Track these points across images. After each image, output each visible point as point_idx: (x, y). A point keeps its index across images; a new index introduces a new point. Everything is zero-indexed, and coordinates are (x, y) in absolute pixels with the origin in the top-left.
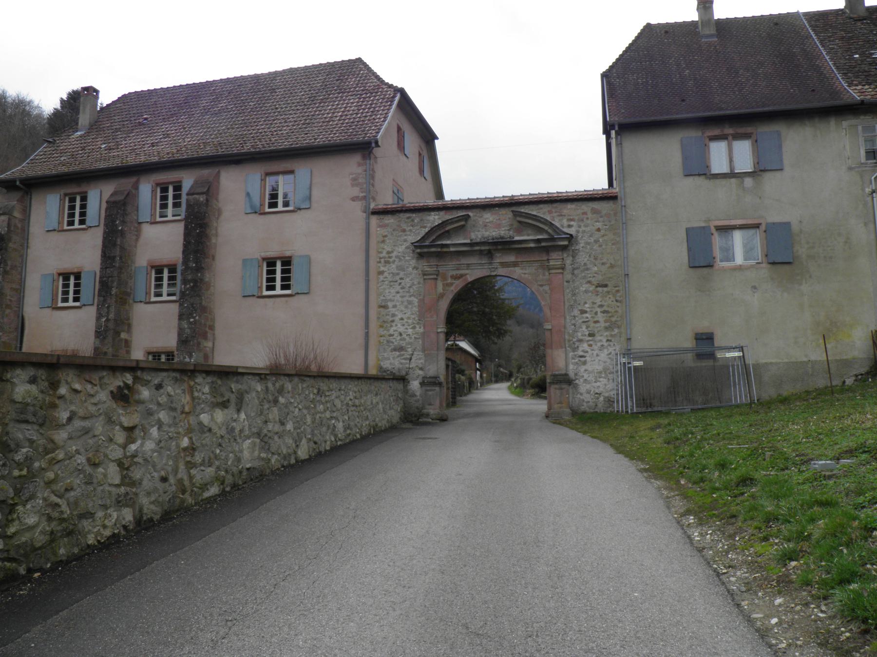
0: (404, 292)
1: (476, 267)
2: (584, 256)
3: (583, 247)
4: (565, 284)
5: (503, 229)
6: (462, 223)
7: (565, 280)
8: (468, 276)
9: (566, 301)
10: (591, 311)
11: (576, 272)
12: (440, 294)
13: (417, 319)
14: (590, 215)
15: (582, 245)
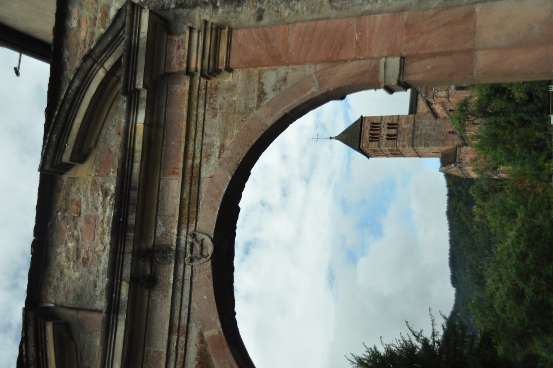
1: (186, 303)
4: (266, 20)
5: (100, 210)
6: (49, 328)
7: (253, 22)
9: (315, 16)
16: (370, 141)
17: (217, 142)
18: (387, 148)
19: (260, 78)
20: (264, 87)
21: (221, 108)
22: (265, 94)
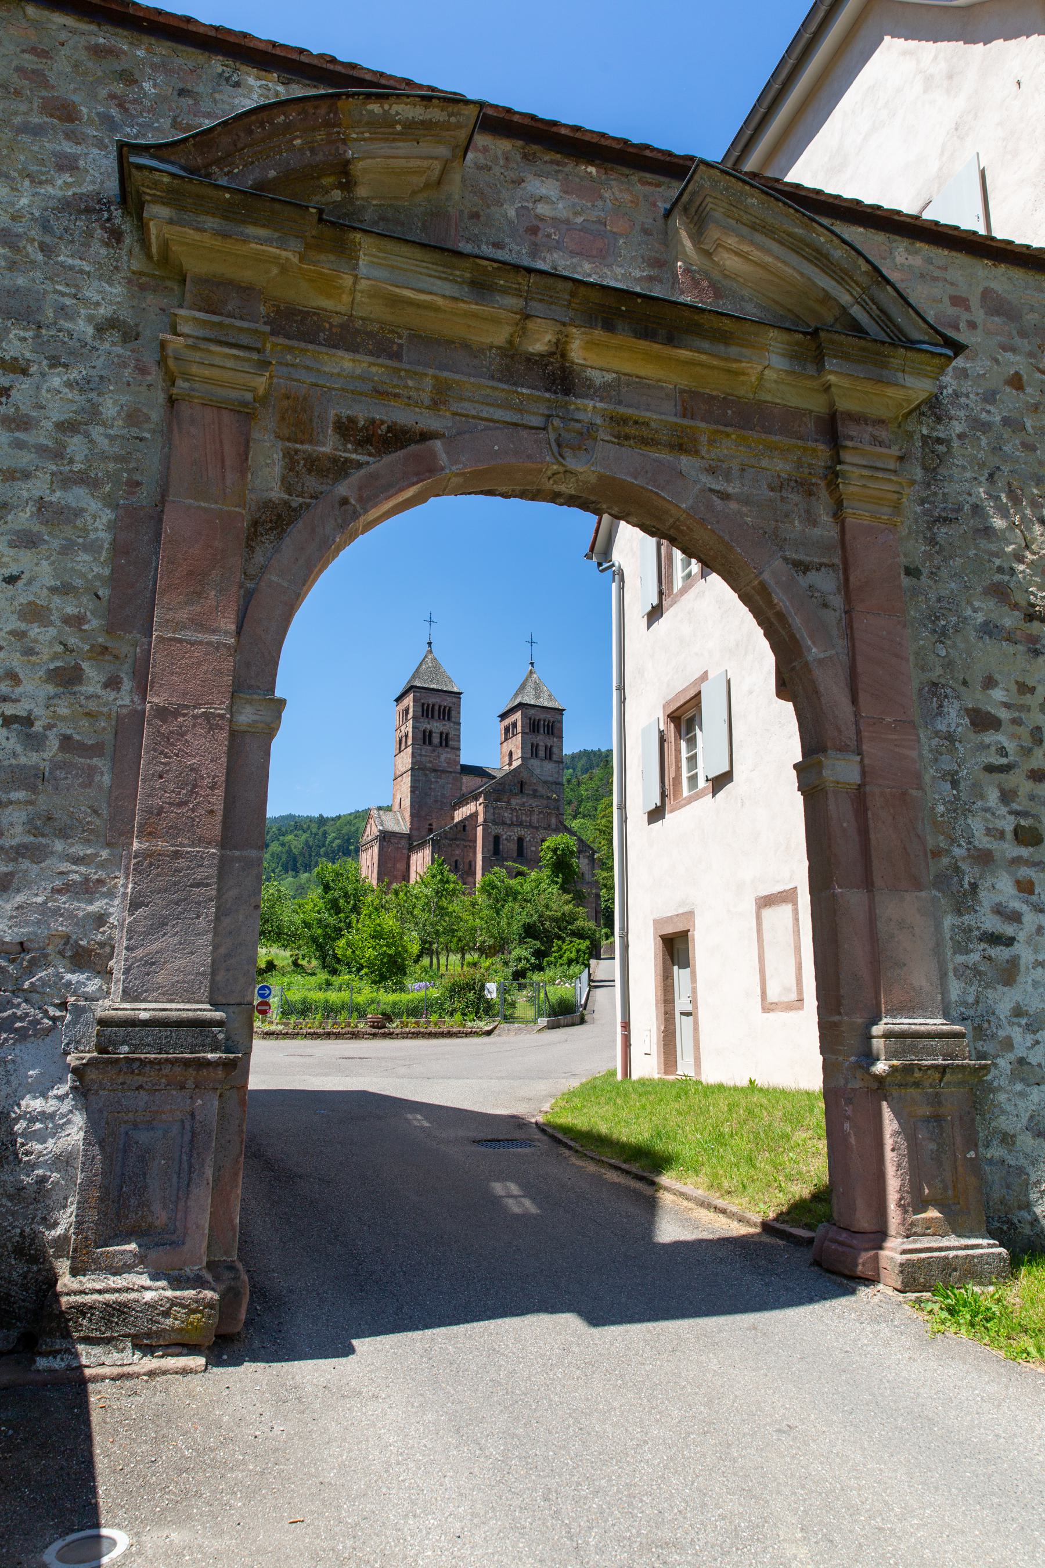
0: (19, 445)
2: (968, 475)
3: (960, 436)
4: (905, 581)
7: (903, 560)
8: (438, 445)
10: (1014, 721)
11: (942, 532)
12: (267, 505)
13: (94, 624)
14: (979, 315)
15: (958, 428)
16: (423, 704)
17: (734, 488)
18: (410, 730)
19: (826, 565)
20: (814, 572)
21: (782, 499)
22: (804, 573)
